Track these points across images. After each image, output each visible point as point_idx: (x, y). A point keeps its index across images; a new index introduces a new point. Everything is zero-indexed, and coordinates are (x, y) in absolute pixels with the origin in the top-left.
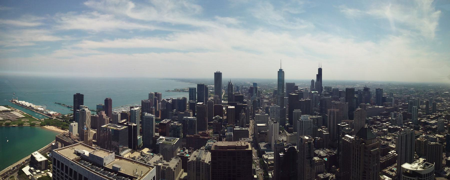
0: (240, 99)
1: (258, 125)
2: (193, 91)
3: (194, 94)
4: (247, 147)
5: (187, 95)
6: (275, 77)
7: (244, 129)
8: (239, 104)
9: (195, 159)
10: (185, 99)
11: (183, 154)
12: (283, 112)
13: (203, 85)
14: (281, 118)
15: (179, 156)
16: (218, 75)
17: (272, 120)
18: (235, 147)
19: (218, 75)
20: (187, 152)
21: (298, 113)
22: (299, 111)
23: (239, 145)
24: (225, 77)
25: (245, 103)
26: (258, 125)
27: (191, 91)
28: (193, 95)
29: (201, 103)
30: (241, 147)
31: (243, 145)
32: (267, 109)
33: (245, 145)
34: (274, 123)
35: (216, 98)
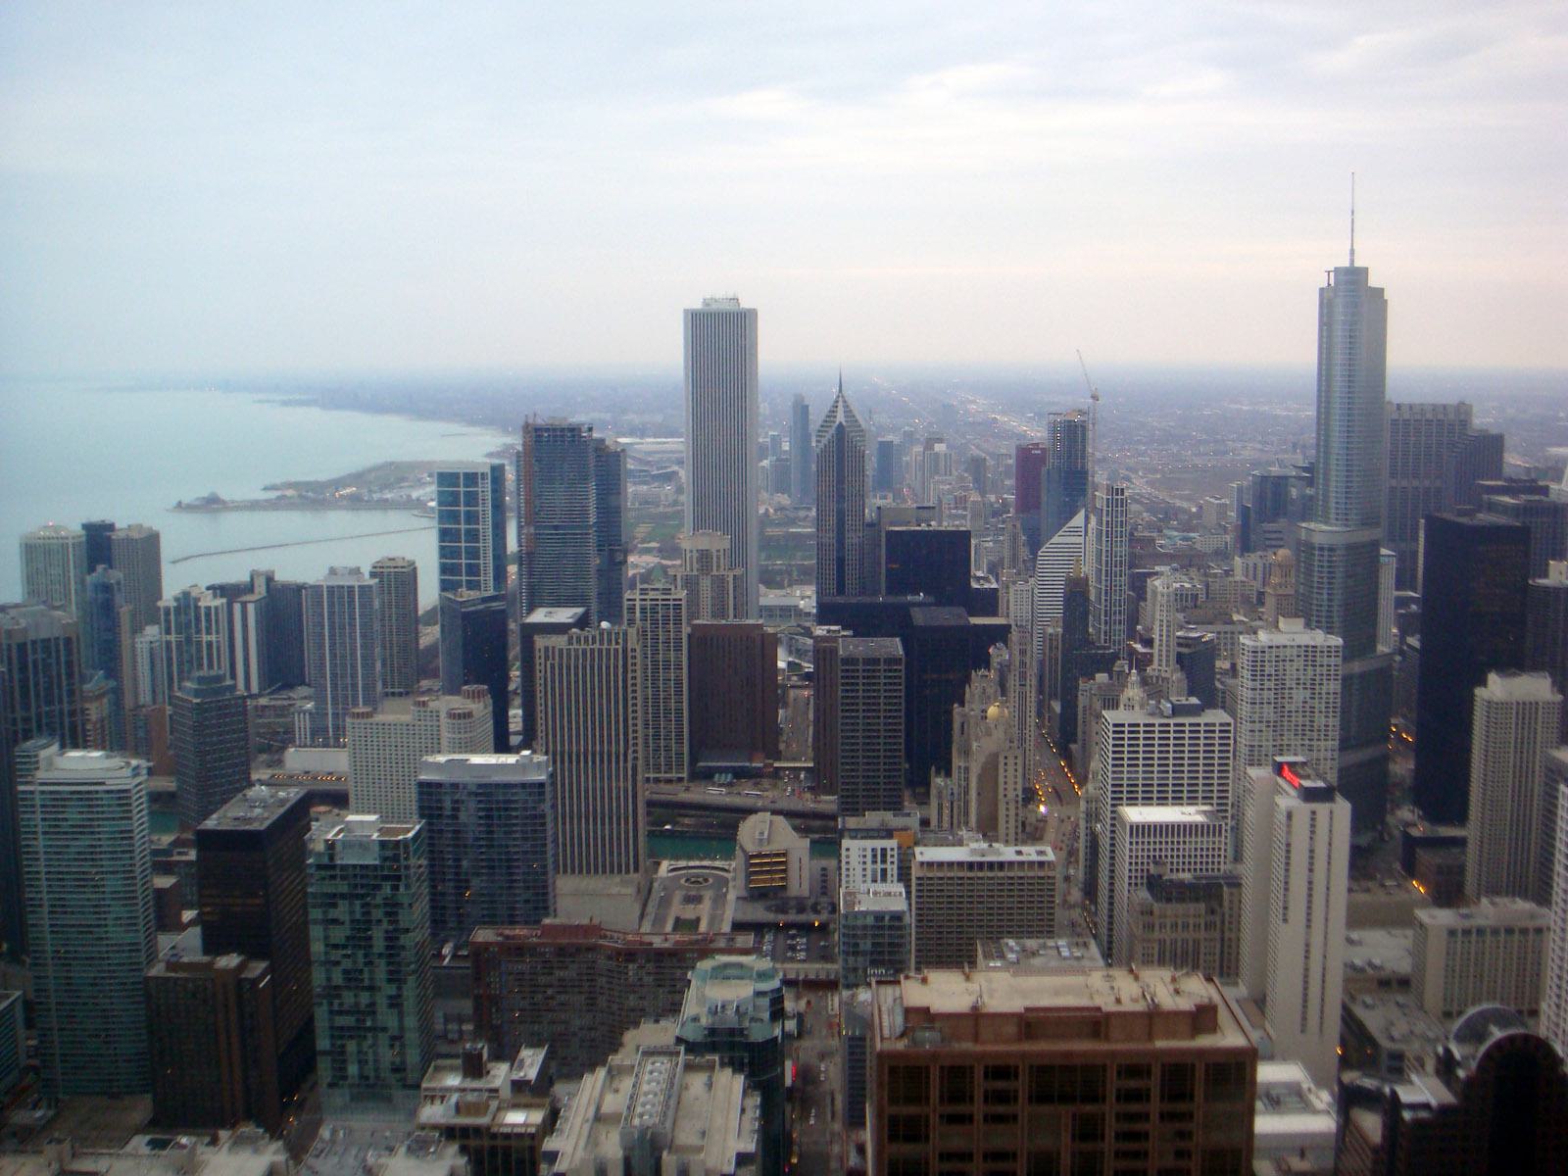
0: (933, 560)
1: (1136, 814)
2: (472, 499)
3: (486, 527)
4: (1203, 1018)
5: (417, 544)
6: (1287, 348)
7: (1007, 853)
8: (923, 609)
9: (612, 1147)
10: (399, 580)
11: (477, 1109)
12: (1364, 705)
13: (574, 430)
14: (1345, 745)
15: (450, 1133)
16: (721, 338)
17: (1279, 768)
18: (1096, 1023)
19: (721, 338)
20: (506, 1093)
21: (1527, 710)
22: (1536, 687)
23: (1128, 1006)
24: (789, 355)
25: (988, 602)
26: (1136, 814)
27: (460, 498)
28: (473, 536)
29: (564, 615)
30: (1153, 1018)
31: (1167, 1000)
32: (1200, 670)
33: (1185, 1004)
34: (1310, 795)
35: (704, 557)
